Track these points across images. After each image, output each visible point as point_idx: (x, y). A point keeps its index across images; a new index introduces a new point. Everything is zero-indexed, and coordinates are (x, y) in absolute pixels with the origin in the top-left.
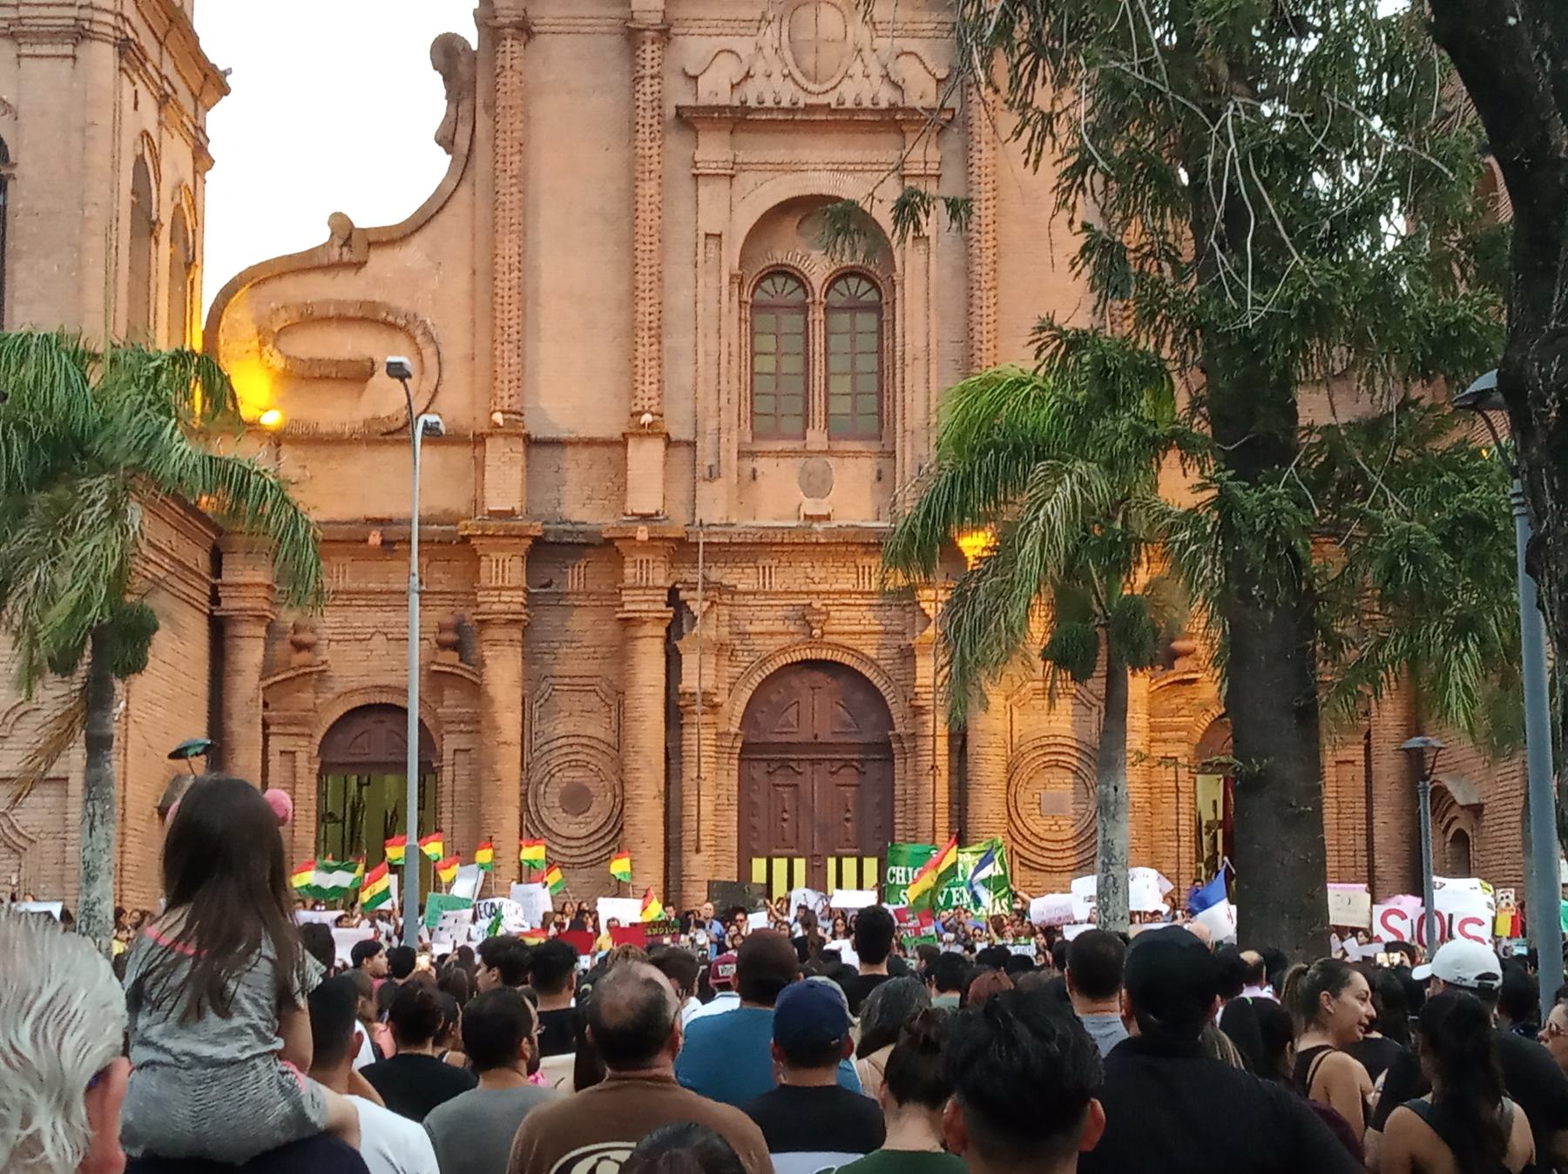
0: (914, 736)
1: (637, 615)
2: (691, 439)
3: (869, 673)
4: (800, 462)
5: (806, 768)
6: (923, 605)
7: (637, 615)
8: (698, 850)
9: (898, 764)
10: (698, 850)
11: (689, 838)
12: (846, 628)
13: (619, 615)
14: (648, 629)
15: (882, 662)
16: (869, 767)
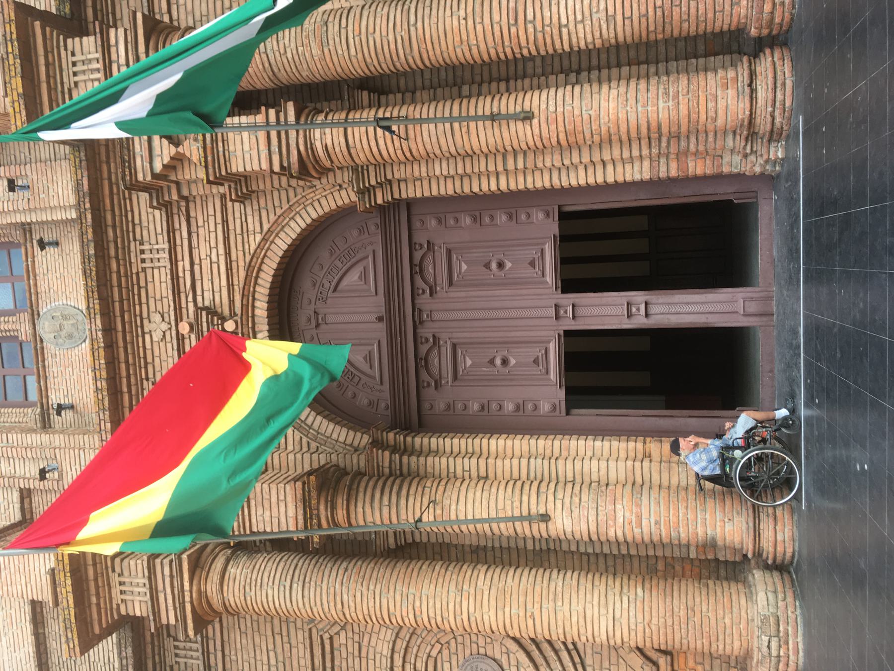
0: (358, 171)
1: (188, 607)
2: (16, 496)
3: (282, 244)
4: (50, 348)
5: (426, 332)
6: (158, 167)
7: (188, 607)
8: (545, 518)
9: (410, 192)
10: (545, 518)
11: (523, 528)
12: (224, 282)
13: (191, 633)
14: (212, 588)
15: (266, 227)
16: (421, 238)
